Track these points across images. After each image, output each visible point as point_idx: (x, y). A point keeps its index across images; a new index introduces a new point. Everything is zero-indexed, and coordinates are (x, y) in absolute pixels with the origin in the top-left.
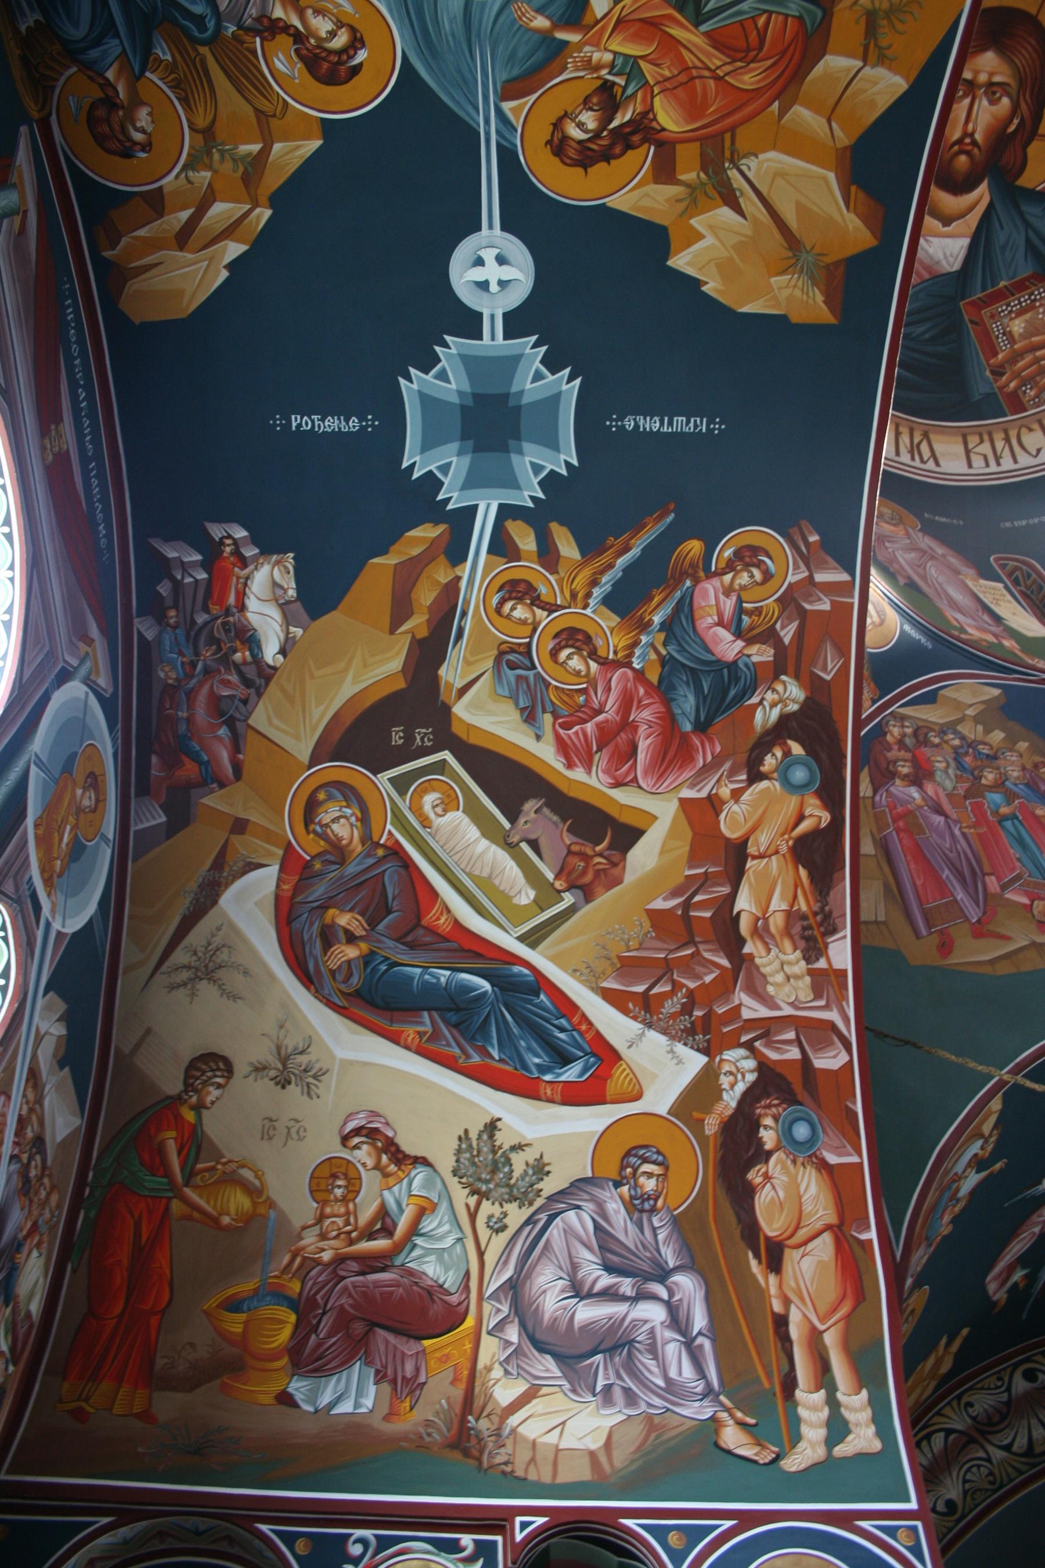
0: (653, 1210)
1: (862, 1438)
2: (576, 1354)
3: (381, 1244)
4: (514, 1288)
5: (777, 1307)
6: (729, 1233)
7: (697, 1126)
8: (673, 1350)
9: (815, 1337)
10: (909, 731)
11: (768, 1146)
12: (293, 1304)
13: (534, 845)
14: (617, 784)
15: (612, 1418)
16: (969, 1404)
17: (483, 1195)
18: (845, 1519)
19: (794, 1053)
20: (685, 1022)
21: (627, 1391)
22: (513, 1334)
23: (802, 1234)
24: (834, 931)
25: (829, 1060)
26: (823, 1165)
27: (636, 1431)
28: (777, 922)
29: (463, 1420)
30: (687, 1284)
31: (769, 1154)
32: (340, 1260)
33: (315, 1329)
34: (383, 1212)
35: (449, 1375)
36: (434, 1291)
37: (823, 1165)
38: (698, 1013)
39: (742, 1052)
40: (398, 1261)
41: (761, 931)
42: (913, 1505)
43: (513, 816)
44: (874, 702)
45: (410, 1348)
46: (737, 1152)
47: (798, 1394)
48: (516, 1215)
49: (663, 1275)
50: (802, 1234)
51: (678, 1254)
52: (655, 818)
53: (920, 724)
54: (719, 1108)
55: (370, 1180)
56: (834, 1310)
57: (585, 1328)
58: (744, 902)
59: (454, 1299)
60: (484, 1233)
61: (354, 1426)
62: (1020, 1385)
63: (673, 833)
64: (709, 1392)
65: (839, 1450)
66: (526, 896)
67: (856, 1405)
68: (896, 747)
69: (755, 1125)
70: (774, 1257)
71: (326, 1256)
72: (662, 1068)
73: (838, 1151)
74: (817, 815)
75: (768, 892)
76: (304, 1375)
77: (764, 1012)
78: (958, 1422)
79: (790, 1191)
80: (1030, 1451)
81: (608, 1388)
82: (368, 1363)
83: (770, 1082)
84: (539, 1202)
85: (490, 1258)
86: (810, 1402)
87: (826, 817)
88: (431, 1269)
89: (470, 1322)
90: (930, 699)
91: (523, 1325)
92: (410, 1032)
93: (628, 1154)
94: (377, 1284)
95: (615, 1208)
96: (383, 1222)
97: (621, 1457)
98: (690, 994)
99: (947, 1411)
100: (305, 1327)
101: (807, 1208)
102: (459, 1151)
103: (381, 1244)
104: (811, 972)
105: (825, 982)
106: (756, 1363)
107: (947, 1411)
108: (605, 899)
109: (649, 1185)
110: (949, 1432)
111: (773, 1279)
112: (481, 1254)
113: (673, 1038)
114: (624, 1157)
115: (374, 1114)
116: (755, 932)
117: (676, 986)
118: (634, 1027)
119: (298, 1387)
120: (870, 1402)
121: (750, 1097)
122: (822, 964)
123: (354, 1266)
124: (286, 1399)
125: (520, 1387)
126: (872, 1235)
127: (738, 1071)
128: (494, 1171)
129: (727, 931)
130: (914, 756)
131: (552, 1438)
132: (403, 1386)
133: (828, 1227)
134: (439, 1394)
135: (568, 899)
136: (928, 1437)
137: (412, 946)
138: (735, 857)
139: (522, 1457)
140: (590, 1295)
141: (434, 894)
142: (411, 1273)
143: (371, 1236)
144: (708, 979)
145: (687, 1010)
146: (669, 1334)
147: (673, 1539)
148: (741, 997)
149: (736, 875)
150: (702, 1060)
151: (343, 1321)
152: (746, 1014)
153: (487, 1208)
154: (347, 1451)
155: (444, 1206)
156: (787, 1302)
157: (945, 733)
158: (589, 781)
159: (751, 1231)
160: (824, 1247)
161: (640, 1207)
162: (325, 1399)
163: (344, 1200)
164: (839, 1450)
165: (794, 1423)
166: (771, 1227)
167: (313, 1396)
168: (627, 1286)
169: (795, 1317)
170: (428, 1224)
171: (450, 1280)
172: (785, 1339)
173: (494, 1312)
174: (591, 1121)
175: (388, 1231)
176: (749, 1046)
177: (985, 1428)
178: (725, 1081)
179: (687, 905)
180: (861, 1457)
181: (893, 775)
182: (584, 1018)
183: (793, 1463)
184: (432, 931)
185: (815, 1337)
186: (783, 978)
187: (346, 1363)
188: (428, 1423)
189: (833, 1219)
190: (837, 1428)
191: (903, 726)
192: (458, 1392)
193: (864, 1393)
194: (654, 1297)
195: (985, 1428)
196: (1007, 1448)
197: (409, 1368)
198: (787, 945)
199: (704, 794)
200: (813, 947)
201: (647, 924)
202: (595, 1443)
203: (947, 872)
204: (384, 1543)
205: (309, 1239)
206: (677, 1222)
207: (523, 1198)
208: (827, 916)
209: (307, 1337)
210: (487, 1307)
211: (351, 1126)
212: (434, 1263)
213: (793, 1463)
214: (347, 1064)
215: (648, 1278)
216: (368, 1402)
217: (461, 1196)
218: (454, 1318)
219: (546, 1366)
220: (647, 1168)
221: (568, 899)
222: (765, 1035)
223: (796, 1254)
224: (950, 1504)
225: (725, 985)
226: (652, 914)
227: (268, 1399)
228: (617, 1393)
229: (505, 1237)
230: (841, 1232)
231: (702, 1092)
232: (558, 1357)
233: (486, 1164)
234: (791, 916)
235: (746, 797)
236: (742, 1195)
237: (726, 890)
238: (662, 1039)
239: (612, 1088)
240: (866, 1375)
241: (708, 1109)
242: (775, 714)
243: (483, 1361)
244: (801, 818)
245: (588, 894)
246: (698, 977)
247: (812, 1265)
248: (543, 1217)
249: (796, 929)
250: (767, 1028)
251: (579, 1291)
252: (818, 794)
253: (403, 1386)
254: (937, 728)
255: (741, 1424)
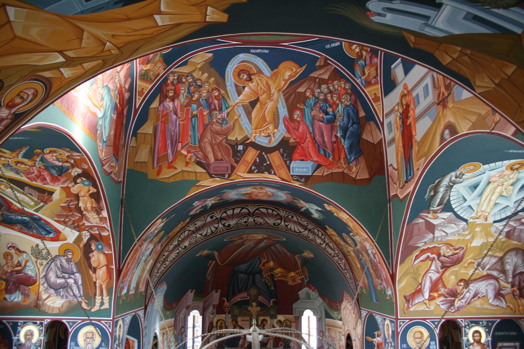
0: (71, 261)
1: (106, 306)
2: (56, 288)
3: (19, 268)
4: (46, 276)
5: (94, 280)
6: (86, 265)
7: (79, 245)
8: (75, 288)
9: (101, 286)
10: (176, 77)
11: (93, 249)
12: (5, 280)
13: (30, 194)
14: (45, 184)
15: (63, 301)
16: (196, 224)
17: (38, 258)
18: (99, 321)
19: (97, 232)
20: (73, 226)
21: (66, 296)
22: (46, 285)
23: (100, 266)
24: (102, 210)
25: (105, 234)
26: (104, 253)
27: (67, 303)
28: (89, 209)
29: (37, 302)
30: (78, 276)
31: (93, 251)
32: (12, 271)
33: (9, 285)
34: (19, 262)
35: (34, 293)
36: (30, 277)
37: (104, 253)
38: (76, 224)
39: (86, 232)
40: (23, 271)
41: (86, 210)
42: (111, 318)
43: (23, 190)
44: (164, 69)
45: (27, 288)
46: (87, 250)
47: (97, 297)
48: (45, 262)
49: (73, 274)
50: (100, 266)
51: (76, 270)
52: (56, 190)
53: (180, 74)
54: (83, 242)
55: (15, 256)
56: (105, 281)
57: (59, 284)
58: (81, 205)
59: (34, 278)
60: (39, 266)
61: (18, 304)
62: (209, 219)
63: (61, 193)
64: (81, 296)
65: (102, 308)
66: (33, 203)
67: (106, 299)
68: (170, 85)
69: (90, 245)
70: (95, 270)
71: (9, 271)
72: (70, 235)
73: (107, 251)
74: (93, 190)
75: (86, 203)
76: (8, 294)
77: (90, 224)
78: (192, 228)
79: (98, 258)
80: (206, 235)
81: (63, 295)
82: (20, 291)
83: (93, 237)
84: (49, 260)
85: (41, 270)
86: (98, 298)
87: (95, 191)
88: (30, 273)
89: (38, 283)
90: (185, 64)
91: (48, 283)
92: (16, 228)
93: (65, 251)
94: (20, 276)
95: (64, 261)
96: (19, 264)
97: (64, 308)
98: (73, 221)
99: (190, 226)
100: (7, 285)
101: (101, 261)
102: (32, 250)
103: (19, 268)
104: (99, 217)
105: (102, 219)
106: (90, 290)
107: (190, 226)
108: (50, 204)
109: (70, 257)
110: (189, 231)
111: (94, 275)
112: (39, 270)
113: (71, 229)
114: (65, 251)
115: (13, 243)
116: (85, 210)
117: (70, 220)
118: (63, 227)
119: (7, 296)
120: (109, 299)
121: (89, 240)
122: (101, 216)
123: (15, 273)
124: (5, 299)
125: (47, 295)
126: (114, 267)
127: (86, 236)
128: (39, 254)
129: (79, 209)
130: (175, 88)
131: (52, 305)
132: (26, 295)
133: (105, 265)
134: (33, 297)
135: (42, 204)
136: (184, 232)
137: (11, 212)
138: (77, 197)
139: (47, 308)
140: (60, 278)
141: (12, 203)
142: (26, 274)
143: (17, 267)
144: (77, 218)
145: (74, 223)
146: (74, 285)
147: (71, 324)
148: (84, 221)
149: (78, 200)
150: (78, 233)
151: (14, 283)
152: (86, 225)
153: (39, 261)
154: (17, 309)
155: (30, 261)
156: (96, 279)
157: (188, 77)
158: (38, 183)
159: (90, 266)
160: (104, 269)
161: (68, 261)
162: (12, 298)
163: (11, 260)
164: (102, 308)
165: (95, 302)
166: (94, 265)
167: (10, 299)
168: (66, 276)
169: (98, 282)
170: (28, 264)
171: (33, 275)
172: (95, 286)
173: (42, 281)
174: (57, 245)
175: (20, 266)
176: (88, 230)
177: (198, 230)
178: (83, 237)
179: (68, 205)
180: (105, 309)
181: (166, 97)
182: (52, 225)
183: (93, 310)
184: (14, 209)
185: (101, 286)
186: (93, 219)
187: (15, 291)
188: (31, 303)
189: (106, 264)
190: (102, 303)
191: (174, 76)
192: (36, 296)
193: (108, 297)
194: (71, 278)
195: (198, 230)
196: (201, 234)
197: (27, 292)
198: (93, 212)
199: (65, 186)
200: (98, 213)
201: (61, 208)
202: (60, 306)
203: (169, 141)
204: (24, 323)
205: (5, 268)
206: (76, 264)
207: (46, 259)
208: (100, 208)
209: (7, 287)
210: (41, 280)
211: (9, 246)
212: (30, 271)
213: (93, 310)
214: (5, 234)
215: (71, 274)
216: (20, 299)
217: (34, 259)
218: (34, 282)
219: (52, 291)
220: (69, 253)
221: (42, 204)
222: (91, 228)
223: (99, 270)
224: (185, 247)
225: (81, 219)
226: (61, 207)
227: (2, 299)
228: (64, 296)
229: (43, 267)
230: (107, 266)
231: (79, 239)
232: (54, 289)
233: (37, 253)
234: (92, 208)
235: (75, 186)
236: (88, 259)
237: (76, 202)
238: (69, 229)
239: (60, 238)
240: (109, 294)
241: (81, 242)
242: (76, 174)
243: (40, 290)
244: (89, 190)
245: (46, 204)
246: (74, 218)
247: (102, 272)
248: (50, 263)
249: (94, 210)
250: (91, 227)
251: (57, 277)
252: (93, 186)
253: (26, 295)
254: (185, 75)
255: (86, 302)
